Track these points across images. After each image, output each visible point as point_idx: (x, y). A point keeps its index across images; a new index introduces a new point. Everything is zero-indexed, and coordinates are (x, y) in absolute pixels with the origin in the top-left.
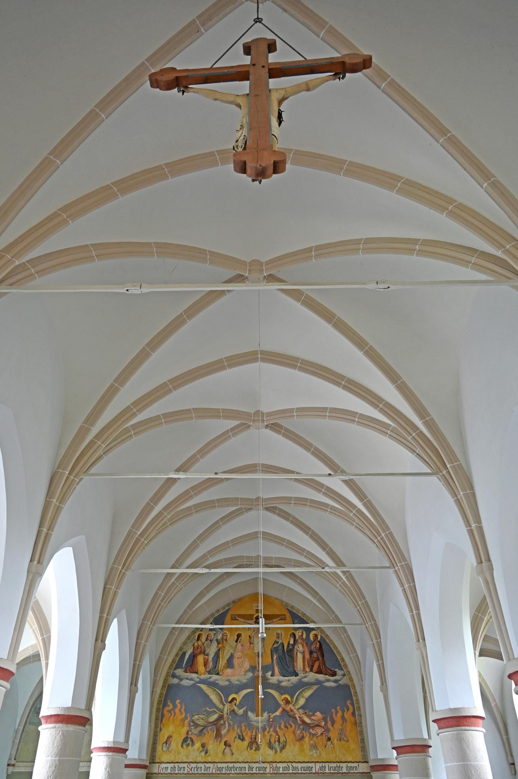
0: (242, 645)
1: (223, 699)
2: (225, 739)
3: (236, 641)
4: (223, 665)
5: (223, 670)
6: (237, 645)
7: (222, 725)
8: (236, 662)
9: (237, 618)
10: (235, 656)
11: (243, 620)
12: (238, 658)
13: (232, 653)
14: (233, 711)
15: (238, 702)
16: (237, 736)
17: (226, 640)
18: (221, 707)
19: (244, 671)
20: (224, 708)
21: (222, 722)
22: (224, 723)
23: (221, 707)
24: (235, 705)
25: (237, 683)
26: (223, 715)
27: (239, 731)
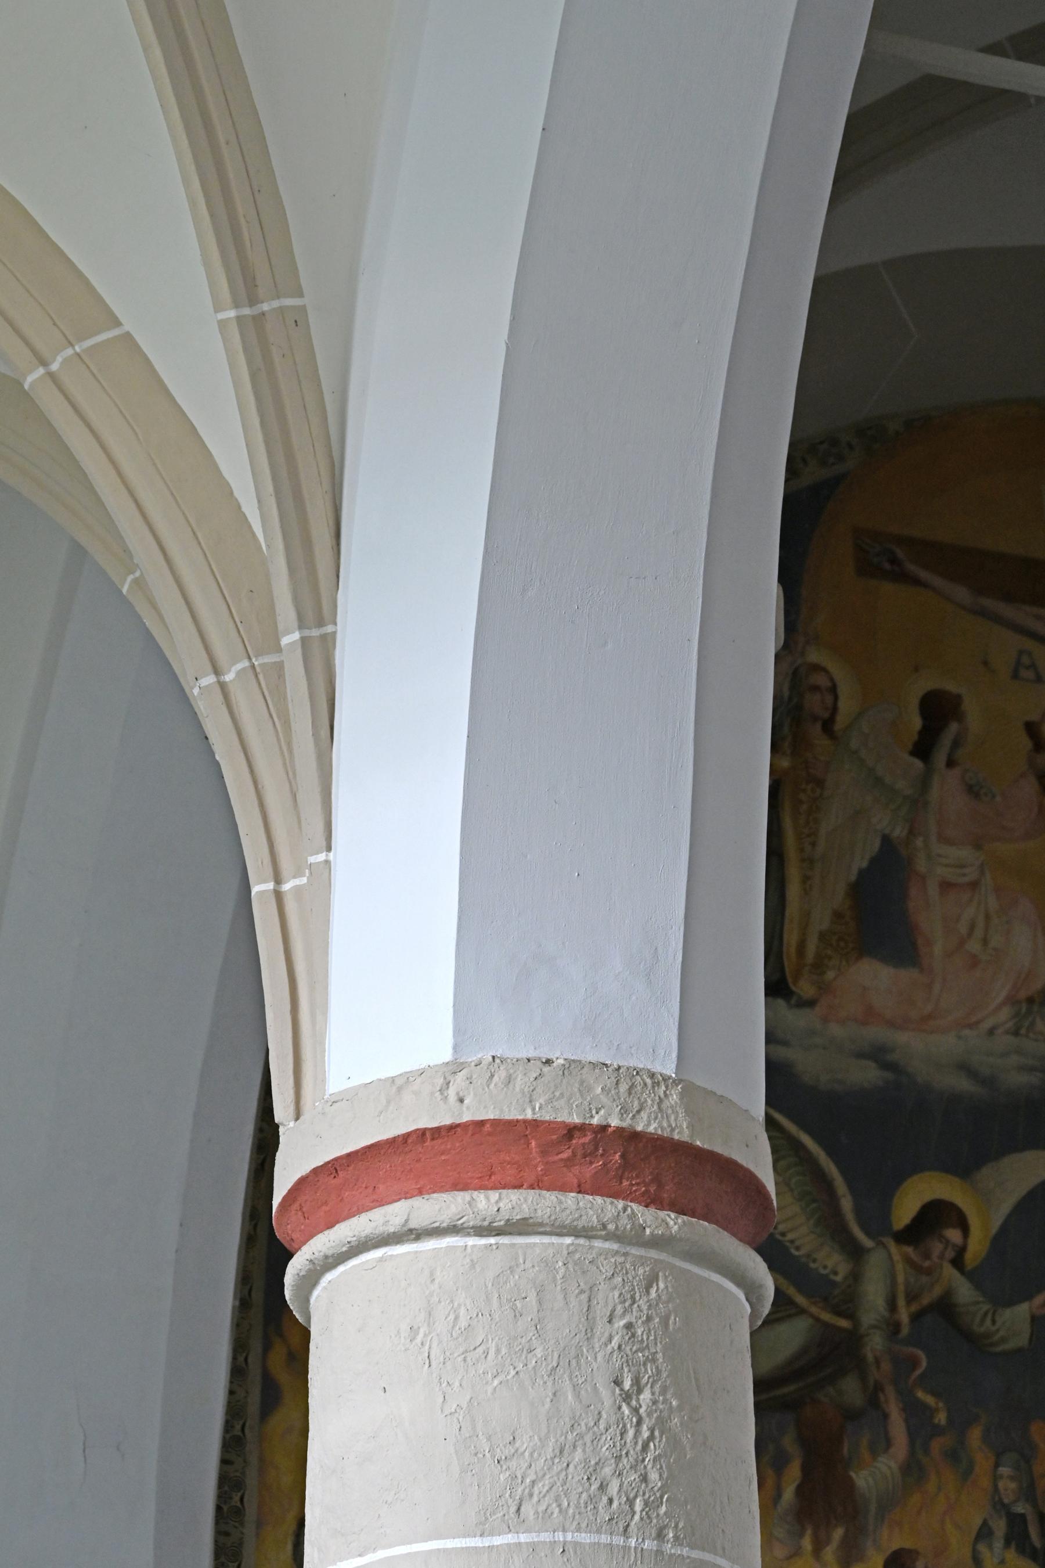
0: (973, 790)
1: (847, 1204)
2: (894, 1540)
3: (923, 749)
4: (821, 921)
5: (819, 966)
6: (924, 782)
7: (852, 1415)
8: (932, 915)
9: (912, 568)
10: (921, 865)
11: (962, 593)
12: (946, 886)
13: (886, 840)
14: (945, 1308)
15: (977, 1246)
16: (1000, 1527)
17: (828, 726)
18: (832, 1262)
19: (1011, 1000)
20: (856, 1276)
21: (851, 1390)
22: (874, 1401)
23: (832, 1262)
24: (958, 1262)
25: (964, 1084)
26: (854, 1339)
27: (1008, 1487)
